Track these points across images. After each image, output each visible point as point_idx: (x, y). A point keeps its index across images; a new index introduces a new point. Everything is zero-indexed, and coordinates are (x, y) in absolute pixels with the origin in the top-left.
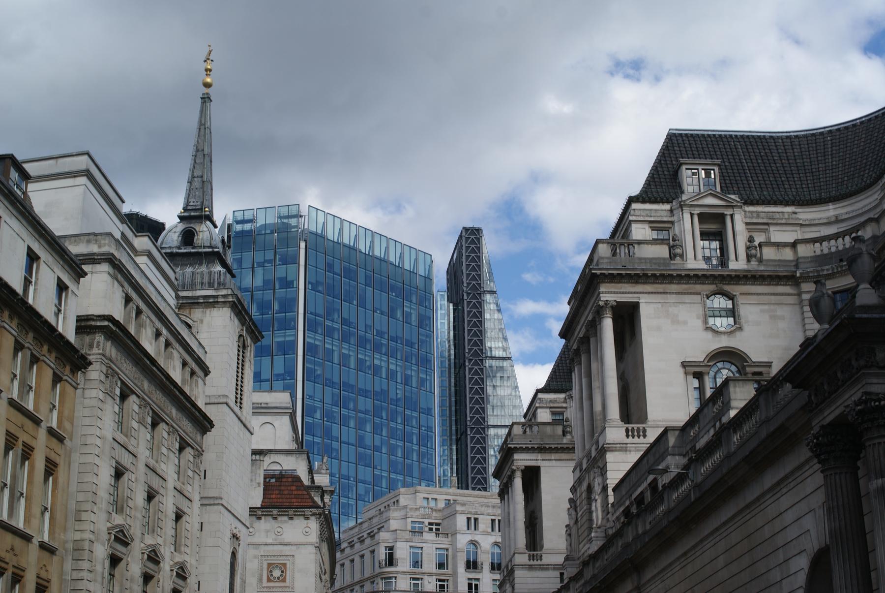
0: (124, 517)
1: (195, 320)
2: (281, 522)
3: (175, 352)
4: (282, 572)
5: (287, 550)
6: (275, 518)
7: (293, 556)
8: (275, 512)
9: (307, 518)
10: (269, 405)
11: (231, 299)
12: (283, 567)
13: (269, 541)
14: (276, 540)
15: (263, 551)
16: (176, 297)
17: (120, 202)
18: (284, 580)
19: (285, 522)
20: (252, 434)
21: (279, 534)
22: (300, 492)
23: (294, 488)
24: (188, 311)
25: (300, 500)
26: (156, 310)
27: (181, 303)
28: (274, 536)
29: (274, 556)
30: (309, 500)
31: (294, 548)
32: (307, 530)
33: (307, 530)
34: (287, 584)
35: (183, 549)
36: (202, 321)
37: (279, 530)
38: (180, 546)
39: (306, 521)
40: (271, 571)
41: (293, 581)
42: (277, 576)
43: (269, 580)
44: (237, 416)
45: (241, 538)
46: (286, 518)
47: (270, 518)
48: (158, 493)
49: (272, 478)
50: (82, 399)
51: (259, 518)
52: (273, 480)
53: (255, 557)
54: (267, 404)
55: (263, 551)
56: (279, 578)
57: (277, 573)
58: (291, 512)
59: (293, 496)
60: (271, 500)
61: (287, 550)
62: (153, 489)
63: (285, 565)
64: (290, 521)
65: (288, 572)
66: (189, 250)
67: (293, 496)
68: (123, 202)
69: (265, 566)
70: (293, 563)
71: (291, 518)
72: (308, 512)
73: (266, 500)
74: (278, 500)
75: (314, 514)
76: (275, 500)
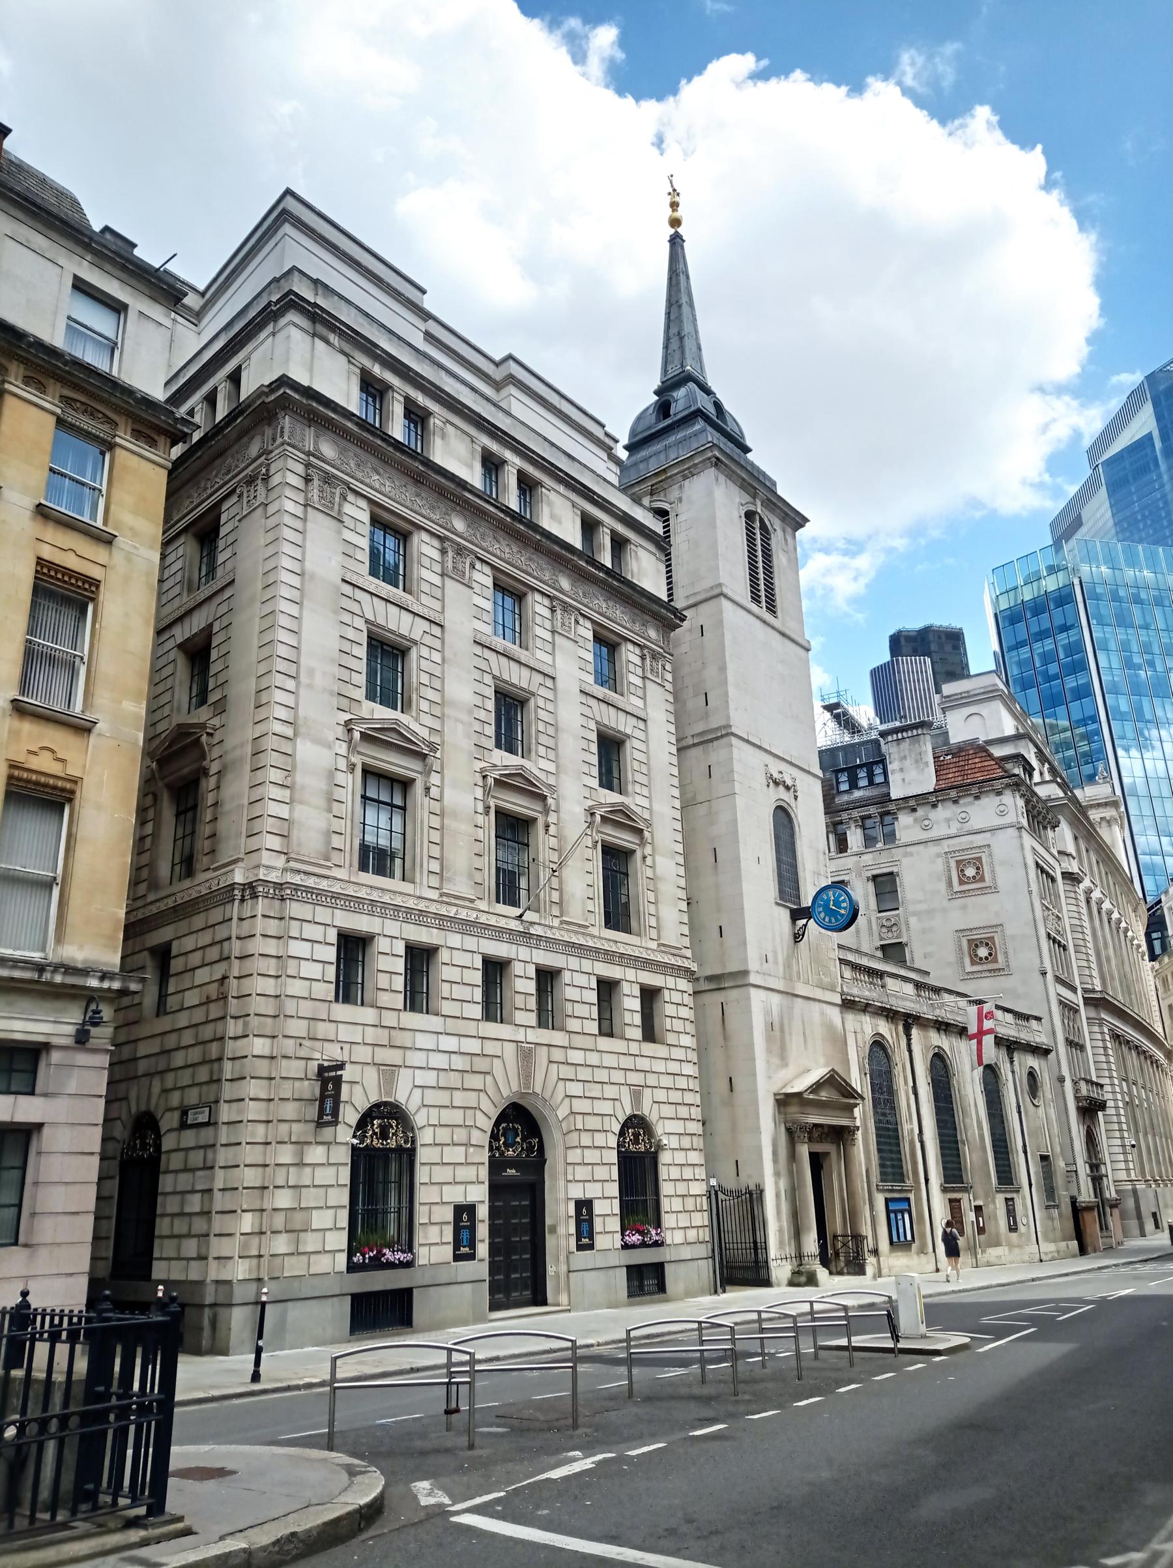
0: (414, 714)
1: (672, 500)
2: (965, 805)
3: (553, 496)
4: (978, 868)
5: (979, 840)
6: (956, 802)
7: (989, 846)
8: (953, 793)
9: (999, 793)
10: (971, 693)
11: (710, 454)
12: (978, 863)
13: (953, 831)
14: (961, 829)
15: (946, 846)
16: (609, 458)
17: (419, 294)
18: (982, 879)
19: (970, 804)
20: (808, 650)
21: (964, 821)
22: (986, 764)
23: (977, 760)
24: (662, 494)
25: (986, 773)
26: (469, 416)
27: (652, 486)
28: (959, 825)
29: (963, 850)
30: (998, 771)
31: (988, 835)
32: (1002, 808)
33: (1002, 808)
34: (988, 883)
35: (630, 788)
36: (680, 500)
37: (963, 815)
38: (626, 784)
39: (998, 798)
40: (962, 871)
41: (994, 879)
42: (971, 876)
43: (961, 882)
44: (757, 617)
45: (798, 788)
46: (970, 799)
47: (949, 804)
48: (533, 694)
49: (947, 755)
50: (263, 520)
51: (934, 806)
52: (949, 757)
53: (938, 855)
54: (968, 692)
55: (946, 846)
56: (974, 877)
57: (970, 872)
58: (975, 790)
59: (976, 770)
60: (947, 781)
61: (979, 840)
62: (379, 626)
63: (979, 859)
64: (977, 802)
65: (985, 867)
66: (668, 421)
67: (976, 770)
68: (424, 292)
69: (953, 864)
70: (990, 855)
71: (977, 798)
72: (998, 784)
73: (941, 782)
74: (957, 779)
75: (1008, 786)
76: (953, 780)
